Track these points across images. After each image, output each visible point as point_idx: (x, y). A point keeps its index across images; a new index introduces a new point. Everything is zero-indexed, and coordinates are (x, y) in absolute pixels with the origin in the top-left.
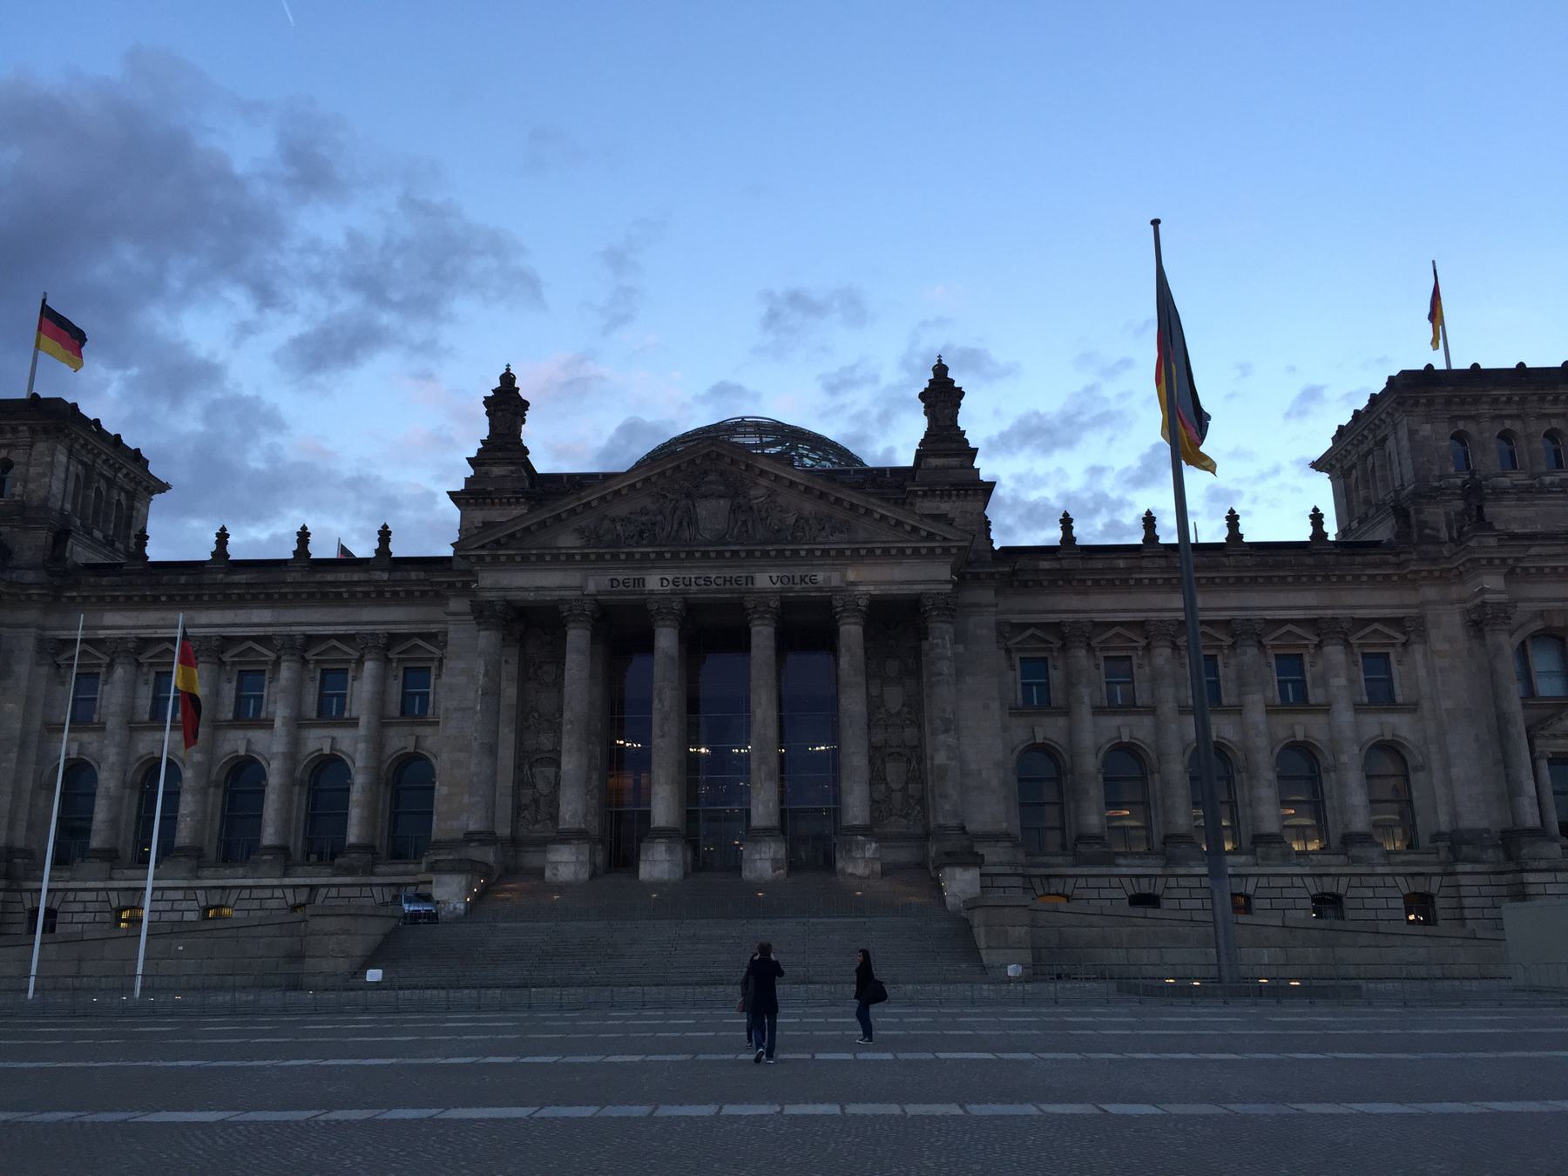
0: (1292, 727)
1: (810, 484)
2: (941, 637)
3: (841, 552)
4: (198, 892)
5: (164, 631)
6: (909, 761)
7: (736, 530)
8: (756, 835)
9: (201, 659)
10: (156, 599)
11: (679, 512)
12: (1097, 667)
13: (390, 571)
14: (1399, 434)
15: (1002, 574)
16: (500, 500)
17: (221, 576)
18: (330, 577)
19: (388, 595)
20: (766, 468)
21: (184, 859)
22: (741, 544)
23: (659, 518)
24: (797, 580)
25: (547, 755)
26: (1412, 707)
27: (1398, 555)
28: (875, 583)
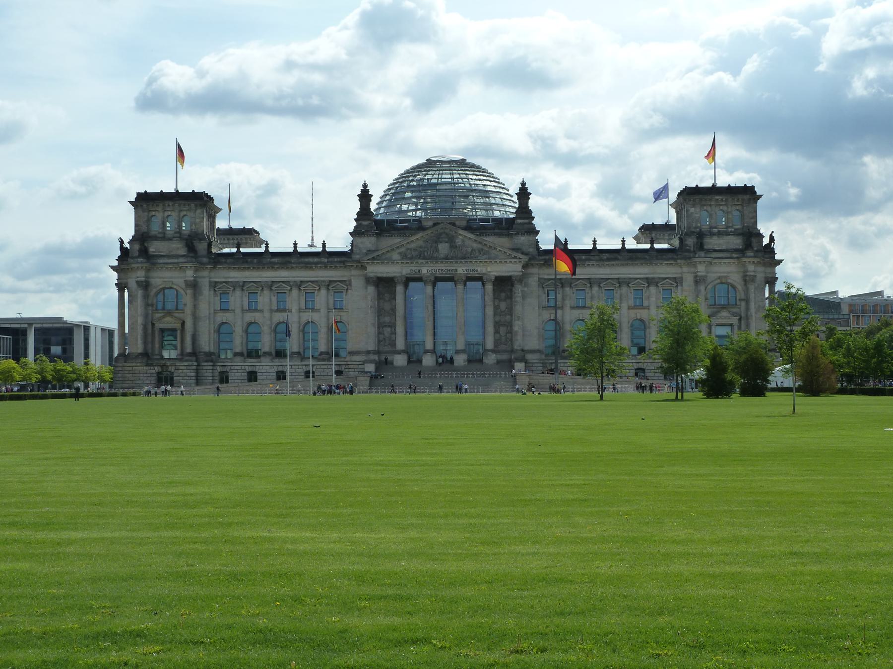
0: (637, 315)
1: (476, 239)
2: (518, 289)
6: (507, 327)
10: (249, 268)
12: (573, 293)
15: (541, 264)
16: (367, 236)
17: (269, 260)
18: (306, 260)
19: (329, 267)
21: (268, 356)
23: (426, 249)
24: (472, 270)
25: (387, 324)
28: (496, 271)
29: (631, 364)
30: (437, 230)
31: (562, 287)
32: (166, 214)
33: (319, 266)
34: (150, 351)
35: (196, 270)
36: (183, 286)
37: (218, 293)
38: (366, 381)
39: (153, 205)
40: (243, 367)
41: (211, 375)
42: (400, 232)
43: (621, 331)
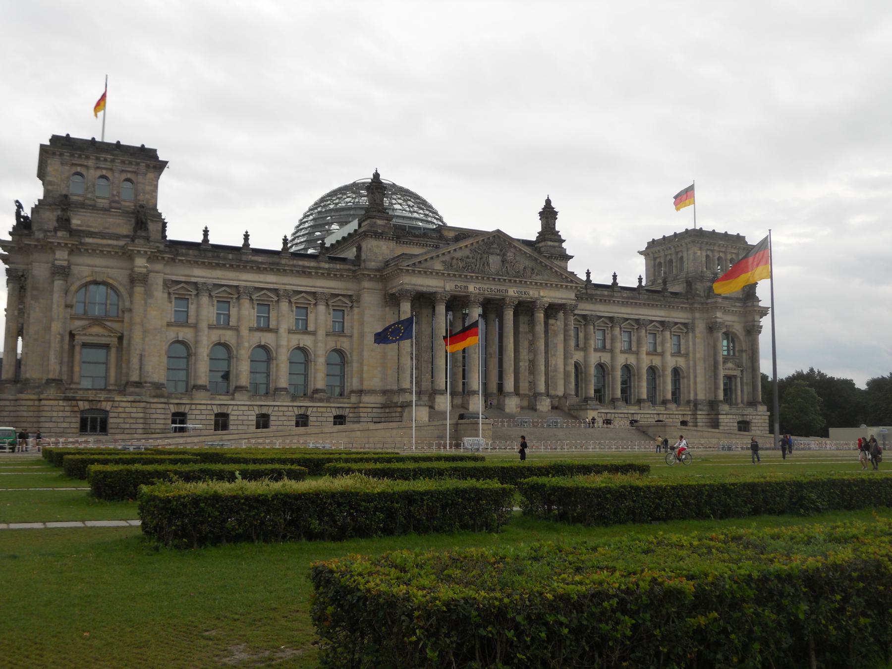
0: (652, 360)
3: (541, 284)
4: (255, 407)
5: (225, 281)
7: (503, 270)
8: (508, 394)
9: (244, 297)
10: (224, 265)
11: (484, 259)
12: (594, 333)
13: (329, 263)
14: (689, 252)
17: (250, 256)
18: (301, 263)
19: (332, 275)
20: (517, 245)
22: (506, 276)
23: (474, 260)
24: (523, 293)
26: (686, 355)
27: (687, 299)
28: (551, 298)
29: (652, 416)
30: (489, 238)
31: (584, 325)
32: (99, 173)
33: (321, 271)
34: (65, 377)
35: (149, 260)
36: (125, 280)
37: (173, 296)
38: (490, 429)
39: (80, 157)
40: (208, 406)
41: (163, 416)
42: (419, 239)
43: (639, 378)
